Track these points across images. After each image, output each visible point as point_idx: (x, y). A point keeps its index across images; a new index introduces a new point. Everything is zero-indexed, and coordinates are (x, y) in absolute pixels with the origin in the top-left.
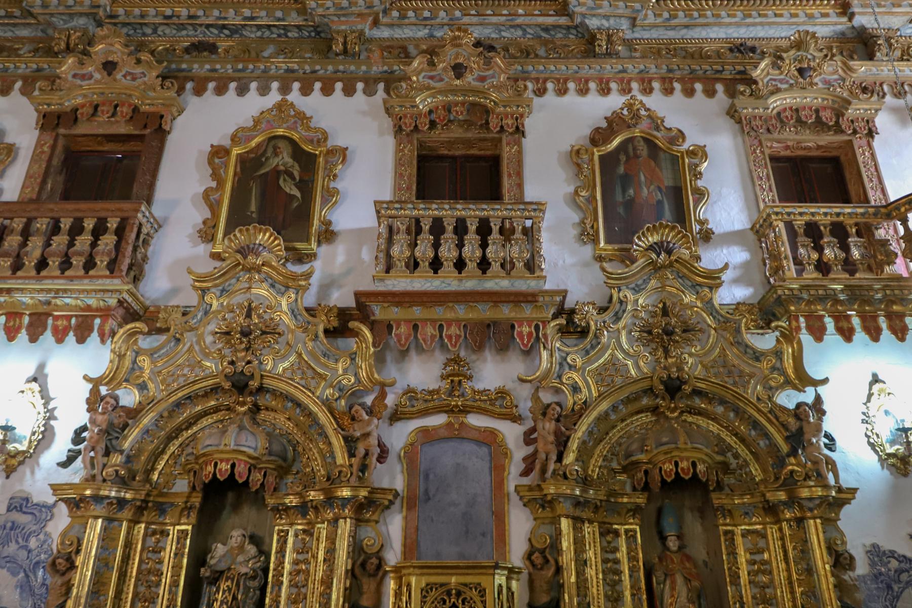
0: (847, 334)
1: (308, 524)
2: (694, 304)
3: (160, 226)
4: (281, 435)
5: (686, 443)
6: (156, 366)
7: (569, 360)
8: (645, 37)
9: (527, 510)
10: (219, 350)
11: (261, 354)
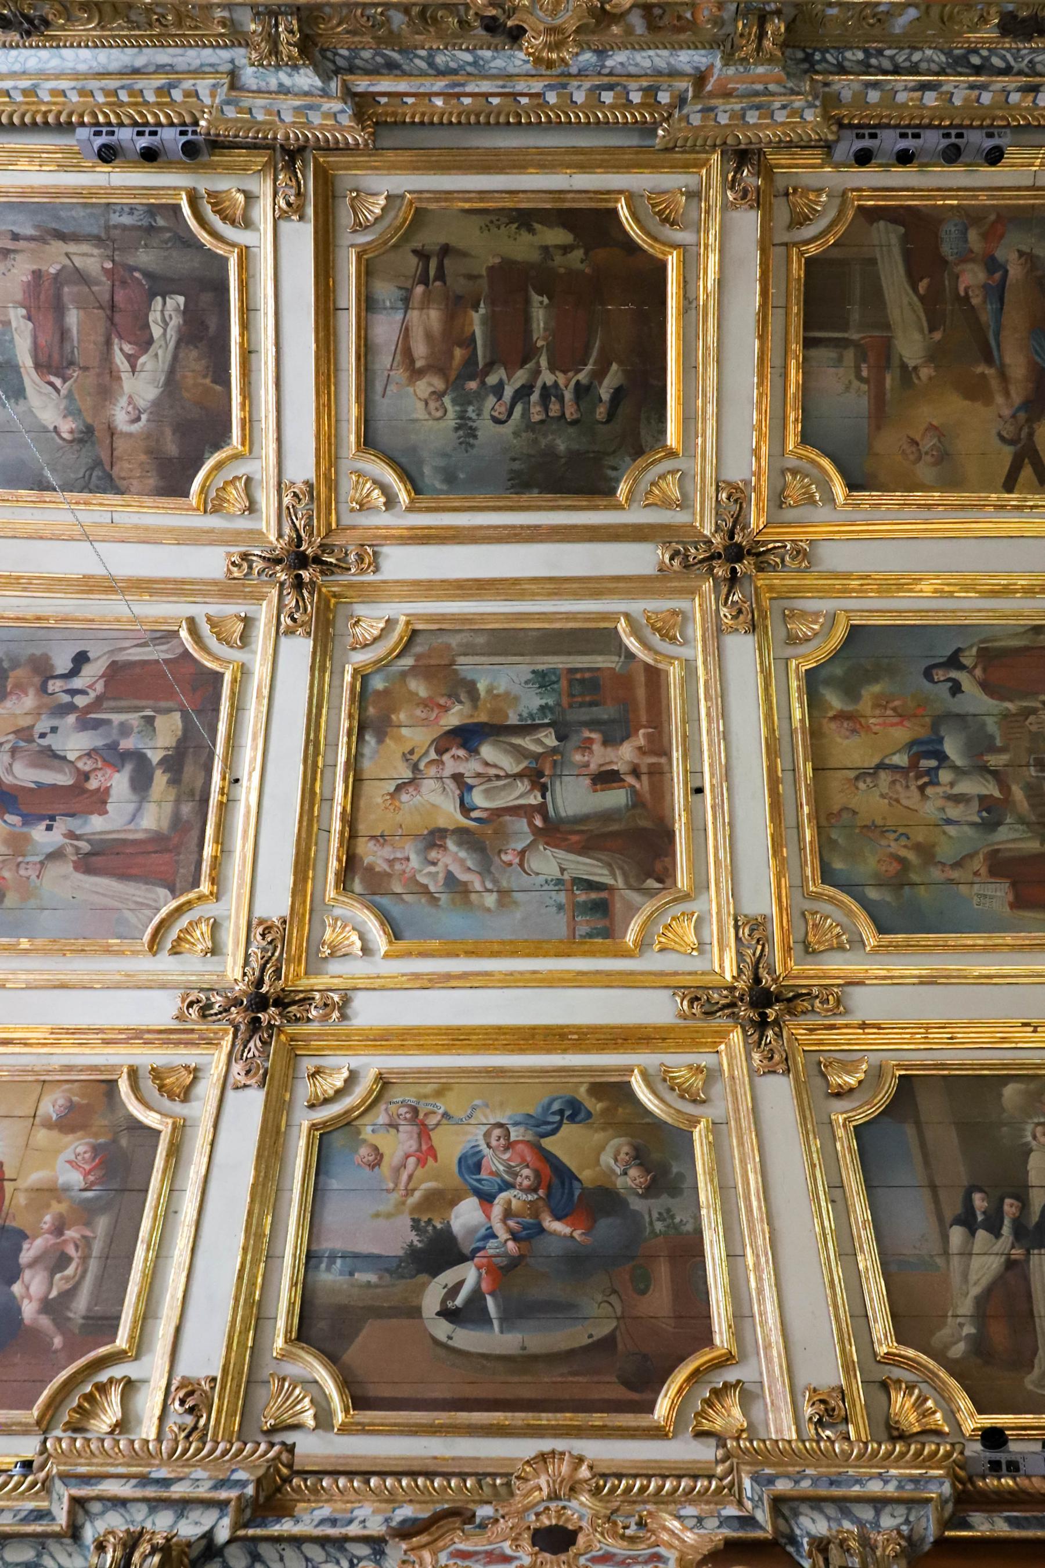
8: (208, 51)
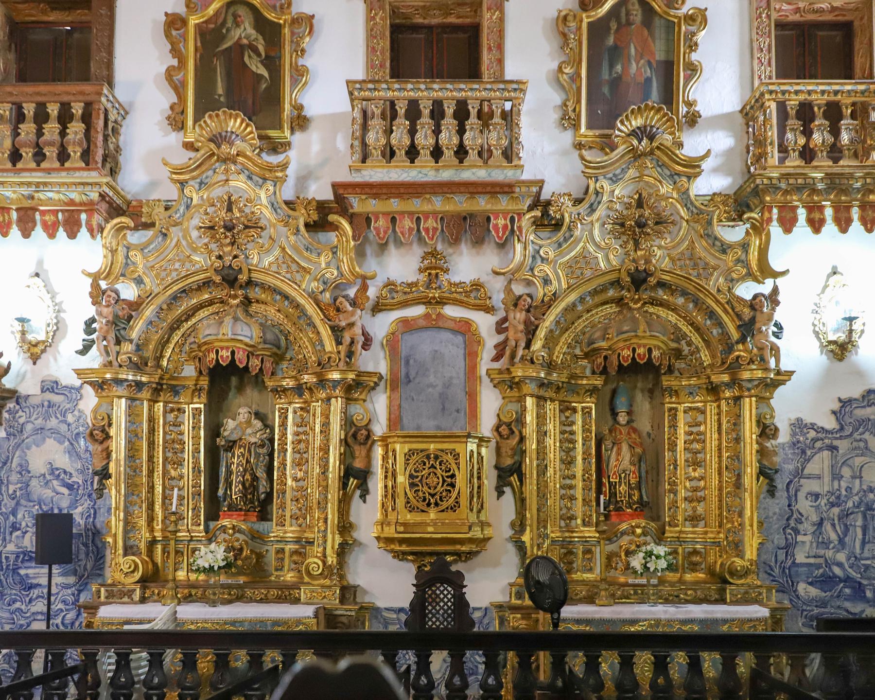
0: (816, 225)
1: (305, 402)
2: (670, 195)
3: (127, 113)
4: (273, 326)
5: (645, 332)
6: (148, 261)
7: (541, 253)
9: (497, 391)
10: (206, 245)
11: (246, 249)
